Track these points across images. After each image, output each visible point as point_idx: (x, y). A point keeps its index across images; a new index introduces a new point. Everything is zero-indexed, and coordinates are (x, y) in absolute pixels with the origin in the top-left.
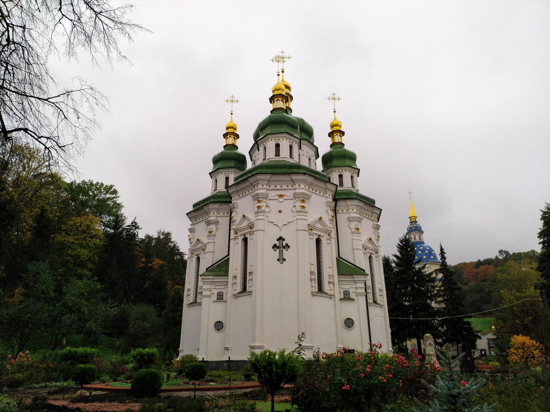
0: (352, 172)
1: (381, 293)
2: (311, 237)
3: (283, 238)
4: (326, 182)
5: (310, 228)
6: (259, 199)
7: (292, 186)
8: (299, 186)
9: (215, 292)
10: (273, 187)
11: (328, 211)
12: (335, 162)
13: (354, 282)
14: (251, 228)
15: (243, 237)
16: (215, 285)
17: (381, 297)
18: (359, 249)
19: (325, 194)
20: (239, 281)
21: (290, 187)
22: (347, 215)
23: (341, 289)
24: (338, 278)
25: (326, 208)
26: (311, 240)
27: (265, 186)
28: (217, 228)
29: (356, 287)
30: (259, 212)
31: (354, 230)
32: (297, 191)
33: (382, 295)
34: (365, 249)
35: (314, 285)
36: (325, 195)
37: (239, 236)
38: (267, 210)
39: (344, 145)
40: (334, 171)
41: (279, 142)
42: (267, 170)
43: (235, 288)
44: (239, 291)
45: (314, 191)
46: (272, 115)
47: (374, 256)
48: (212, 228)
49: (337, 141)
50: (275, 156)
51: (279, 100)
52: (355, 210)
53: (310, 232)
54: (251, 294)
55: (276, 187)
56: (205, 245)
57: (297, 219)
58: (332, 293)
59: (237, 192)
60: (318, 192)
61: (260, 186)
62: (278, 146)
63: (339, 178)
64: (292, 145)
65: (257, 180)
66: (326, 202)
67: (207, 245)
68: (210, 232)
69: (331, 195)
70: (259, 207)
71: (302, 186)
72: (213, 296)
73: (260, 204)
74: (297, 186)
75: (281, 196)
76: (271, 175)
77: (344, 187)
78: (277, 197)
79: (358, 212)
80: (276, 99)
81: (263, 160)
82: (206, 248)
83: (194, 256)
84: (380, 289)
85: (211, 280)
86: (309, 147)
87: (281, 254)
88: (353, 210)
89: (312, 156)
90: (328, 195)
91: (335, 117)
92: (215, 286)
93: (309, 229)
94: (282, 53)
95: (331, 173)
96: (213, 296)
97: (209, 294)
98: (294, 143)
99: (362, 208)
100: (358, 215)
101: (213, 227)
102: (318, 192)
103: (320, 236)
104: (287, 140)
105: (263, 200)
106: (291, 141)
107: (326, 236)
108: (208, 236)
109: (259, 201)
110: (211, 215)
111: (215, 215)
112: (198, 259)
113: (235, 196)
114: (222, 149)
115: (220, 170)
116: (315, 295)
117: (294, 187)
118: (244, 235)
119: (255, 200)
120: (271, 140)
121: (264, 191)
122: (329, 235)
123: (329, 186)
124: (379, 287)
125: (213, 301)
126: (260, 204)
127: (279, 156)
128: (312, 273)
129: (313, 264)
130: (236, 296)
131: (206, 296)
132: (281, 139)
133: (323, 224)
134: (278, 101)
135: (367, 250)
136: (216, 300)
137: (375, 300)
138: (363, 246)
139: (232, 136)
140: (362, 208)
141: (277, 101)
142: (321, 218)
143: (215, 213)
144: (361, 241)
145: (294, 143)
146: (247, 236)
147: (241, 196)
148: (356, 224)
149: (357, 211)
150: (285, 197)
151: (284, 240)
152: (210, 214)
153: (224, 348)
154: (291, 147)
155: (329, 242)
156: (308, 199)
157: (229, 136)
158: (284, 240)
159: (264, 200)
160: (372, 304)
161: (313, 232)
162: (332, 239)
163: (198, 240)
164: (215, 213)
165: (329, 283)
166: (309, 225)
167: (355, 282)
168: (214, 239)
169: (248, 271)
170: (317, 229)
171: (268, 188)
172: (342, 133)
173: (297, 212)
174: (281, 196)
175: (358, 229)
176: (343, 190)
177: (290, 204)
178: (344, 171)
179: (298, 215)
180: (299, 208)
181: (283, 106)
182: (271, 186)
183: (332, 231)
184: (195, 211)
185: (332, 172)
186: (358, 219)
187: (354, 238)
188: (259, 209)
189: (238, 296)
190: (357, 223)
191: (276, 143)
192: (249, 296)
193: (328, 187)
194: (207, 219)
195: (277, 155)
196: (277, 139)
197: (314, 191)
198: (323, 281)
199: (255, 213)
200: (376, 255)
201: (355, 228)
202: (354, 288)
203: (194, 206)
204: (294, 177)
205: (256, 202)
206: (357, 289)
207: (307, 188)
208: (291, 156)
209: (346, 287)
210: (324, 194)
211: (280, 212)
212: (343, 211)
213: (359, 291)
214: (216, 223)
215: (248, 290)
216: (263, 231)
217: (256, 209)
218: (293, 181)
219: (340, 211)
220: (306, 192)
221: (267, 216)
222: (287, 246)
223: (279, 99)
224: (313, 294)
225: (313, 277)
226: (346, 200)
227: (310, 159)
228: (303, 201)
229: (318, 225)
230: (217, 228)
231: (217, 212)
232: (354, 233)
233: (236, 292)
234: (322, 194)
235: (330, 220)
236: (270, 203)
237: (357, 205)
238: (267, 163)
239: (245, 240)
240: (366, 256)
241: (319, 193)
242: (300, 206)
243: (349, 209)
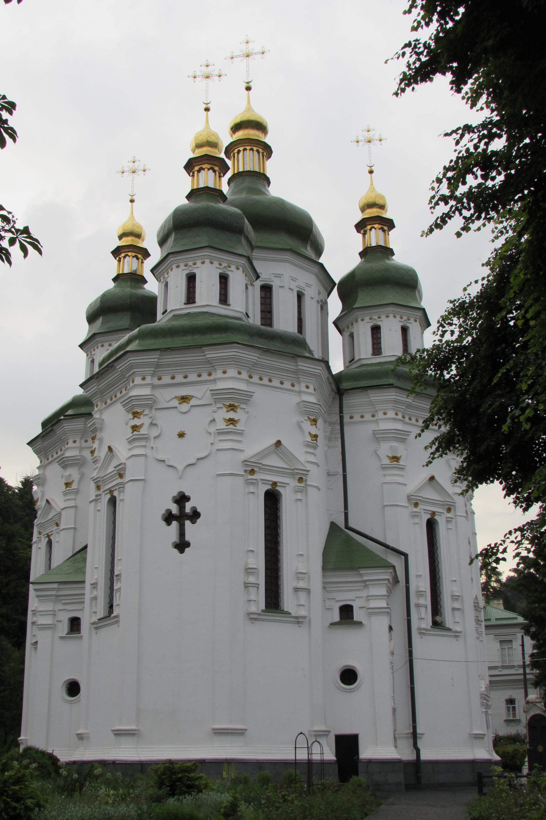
0: (405, 318)
1: (456, 605)
2: (252, 489)
3: (186, 494)
4: (296, 356)
5: (250, 469)
6: (136, 410)
7: (210, 375)
8: (224, 372)
9: (65, 618)
10: (166, 380)
11: (302, 424)
12: (362, 299)
13: (363, 584)
14: (121, 476)
15: (109, 496)
16: (63, 602)
17: (457, 613)
18: (396, 505)
19: (296, 385)
20: (101, 593)
21: (205, 377)
22: (373, 427)
23: (329, 604)
24: (324, 576)
25: (299, 418)
26: (251, 495)
27: (148, 380)
28: (82, 476)
29: (368, 596)
30: (134, 440)
31: (387, 461)
32: (220, 385)
33: (458, 609)
34: (416, 505)
35: (253, 597)
36: (296, 388)
37: (103, 494)
38: (154, 432)
39: (390, 252)
40: (359, 319)
41: (195, 271)
42: (152, 341)
43: (94, 610)
44: (102, 616)
45: (265, 381)
46: (193, 205)
47: (441, 520)
48: (70, 475)
49: (374, 244)
50: (185, 304)
51: (204, 169)
52: (391, 414)
53: (250, 477)
54: (117, 622)
55: (173, 378)
56: (59, 514)
57: (217, 450)
58: (302, 612)
59: (101, 393)
60: (276, 383)
61: (138, 380)
62: (191, 279)
63: (373, 334)
64: (228, 273)
65: (131, 367)
66: (298, 404)
67: (64, 513)
68: (67, 484)
69: (311, 387)
70: (135, 428)
71: (232, 372)
72: (59, 625)
73: (137, 422)
74: (219, 374)
75: (184, 399)
76: (158, 352)
77: (383, 355)
78: (175, 403)
79: (400, 417)
80: (197, 168)
81: (163, 313)
82: (60, 519)
83: (43, 538)
84: (453, 596)
85: (54, 593)
86: (295, 265)
87: (182, 533)
88: (385, 414)
89: (309, 285)
90: (303, 385)
91: (372, 184)
92: (64, 604)
93: (245, 471)
95: (355, 325)
96: (59, 625)
97: (50, 622)
98: (233, 268)
99: (409, 406)
100: (399, 426)
101: (73, 473)
102: (276, 383)
103: (275, 484)
104: (212, 263)
105: (144, 410)
106: (224, 265)
107: (293, 483)
108: (65, 494)
109: (136, 415)
110: (69, 445)
111: (77, 444)
112: (50, 543)
113: (99, 404)
114: (111, 285)
115: (98, 339)
116: (256, 619)
117: (212, 378)
118: (111, 492)
119: (128, 412)
120: (178, 267)
121: (146, 391)
122: (301, 480)
123: (303, 365)
124: (452, 591)
125: (62, 638)
126: (137, 422)
127: (194, 302)
128: (249, 571)
129: (252, 551)
130: (98, 625)
131: (44, 627)
132: (199, 263)
133: (287, 456)
134: (202, 172)
135: (421, 507)
136: (64, 635)
137: (438, 618)
138: (409, 498)
139: (130, 254)
140: (409, 406)
141: (199, 171)
142: (278, 443)
143: (78, 440)
144: (405, 485)
145: (233, 268)
146: (116, 494)
147: (109, 402)
148: (391, 447)
149: (396, 414)
150: (193, 402)
151: (188, 499)
152: (67, 444)
153: (77, 734)
154: (224, 279)
155: (299, 496)
156: (246, 402)
157: (123, 255)
158: (188, 499)
159: (147, 412)
160: (426, 630)
161: (257, 476)
162: (309, 489)
163: (48, 501)
164: (78, 440)
165: (296, 590)
166: (245, 461)
167: (366, 584)
168: (75, 499)
169: (116, 573)
170: (271, 470)
171: (156, 382)
172: (389, 224)
173: (220, 433)
174: (184, 399)
175: (396, 459)
176: (380, 364)
177: (205, 414)
178: (383, 317)
179: (220, 440)
180: (221, 425)
181: (215, 184)
182: (163, 378)
183: (308, 471)
184: (43, 436)
185: (357, 321)
186: (396, 433)
187: (388, 479)
188: (135, 433)
189: (100, 625)
190: (395, 444)
191: (187, 272)
192: (116, 625)
193: (300, 367)
194: (61, 455)
195: (191, 301)
196: (190, 263)
197: (265, 381)
198: (281, 587)
199: (129, 442)
200: (449, 515)
201: (391, 456)
202: (362, 597)
203: (45, 424)
204: (211, 354)
205: (131, 416)
206: (369, 600)
207: (245, 375)
208: (224, 299)
209: (346, 598)
210: (293, 385)
211: (181, 435)
212: (362, 417)
213: (374, 604)
214: (79, 463)
215: (115, 613)
216: (142, 482)
217: (129, 433)
218: (209, 362)
219: (357, 418)
220: (242, 386)
221: (152, 448)
222: (195, 515)
223: (204, 166)
224: (252, 618)
225: (252, 579)
226: (369, 392)
227: (300, 296)
228: (232, 408)
229: (274, 461)
230: (82, 476)
231: (81, 439)
232: (385, 468)
233: (95, 619)
234: (287, 385)
235: (308, 446)
236: (161, 417)
237: (396, 401)
238: (168, 321)
239: (113, 502)
240: (417, 520)
241: (280, 385)
242: (225, 419)
243: (377, 411)
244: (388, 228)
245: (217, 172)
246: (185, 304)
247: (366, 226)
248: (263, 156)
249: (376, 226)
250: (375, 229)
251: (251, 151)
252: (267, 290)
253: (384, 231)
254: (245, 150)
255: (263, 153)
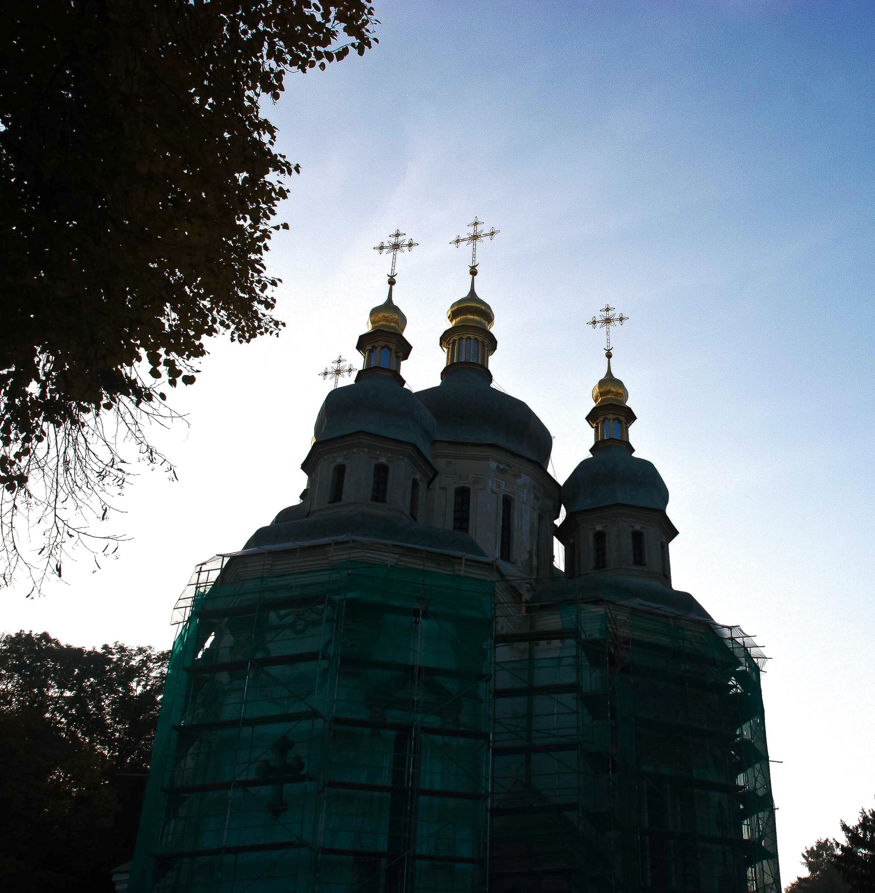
50: (329, 502)
94: (476, 224)
127: (340, 500)
154: (381, 472)
227: (507, 503)
244: (626, 418)
245: (393, 351)
246: (329, 502)
247: (597, 419)
248: (483, 346)
249: (610, 416)
250: (609, 420)
251: (469, 340)
252: (463, 495)
253: (620, 422)
254: (461, 339)
255: (483, 342)
